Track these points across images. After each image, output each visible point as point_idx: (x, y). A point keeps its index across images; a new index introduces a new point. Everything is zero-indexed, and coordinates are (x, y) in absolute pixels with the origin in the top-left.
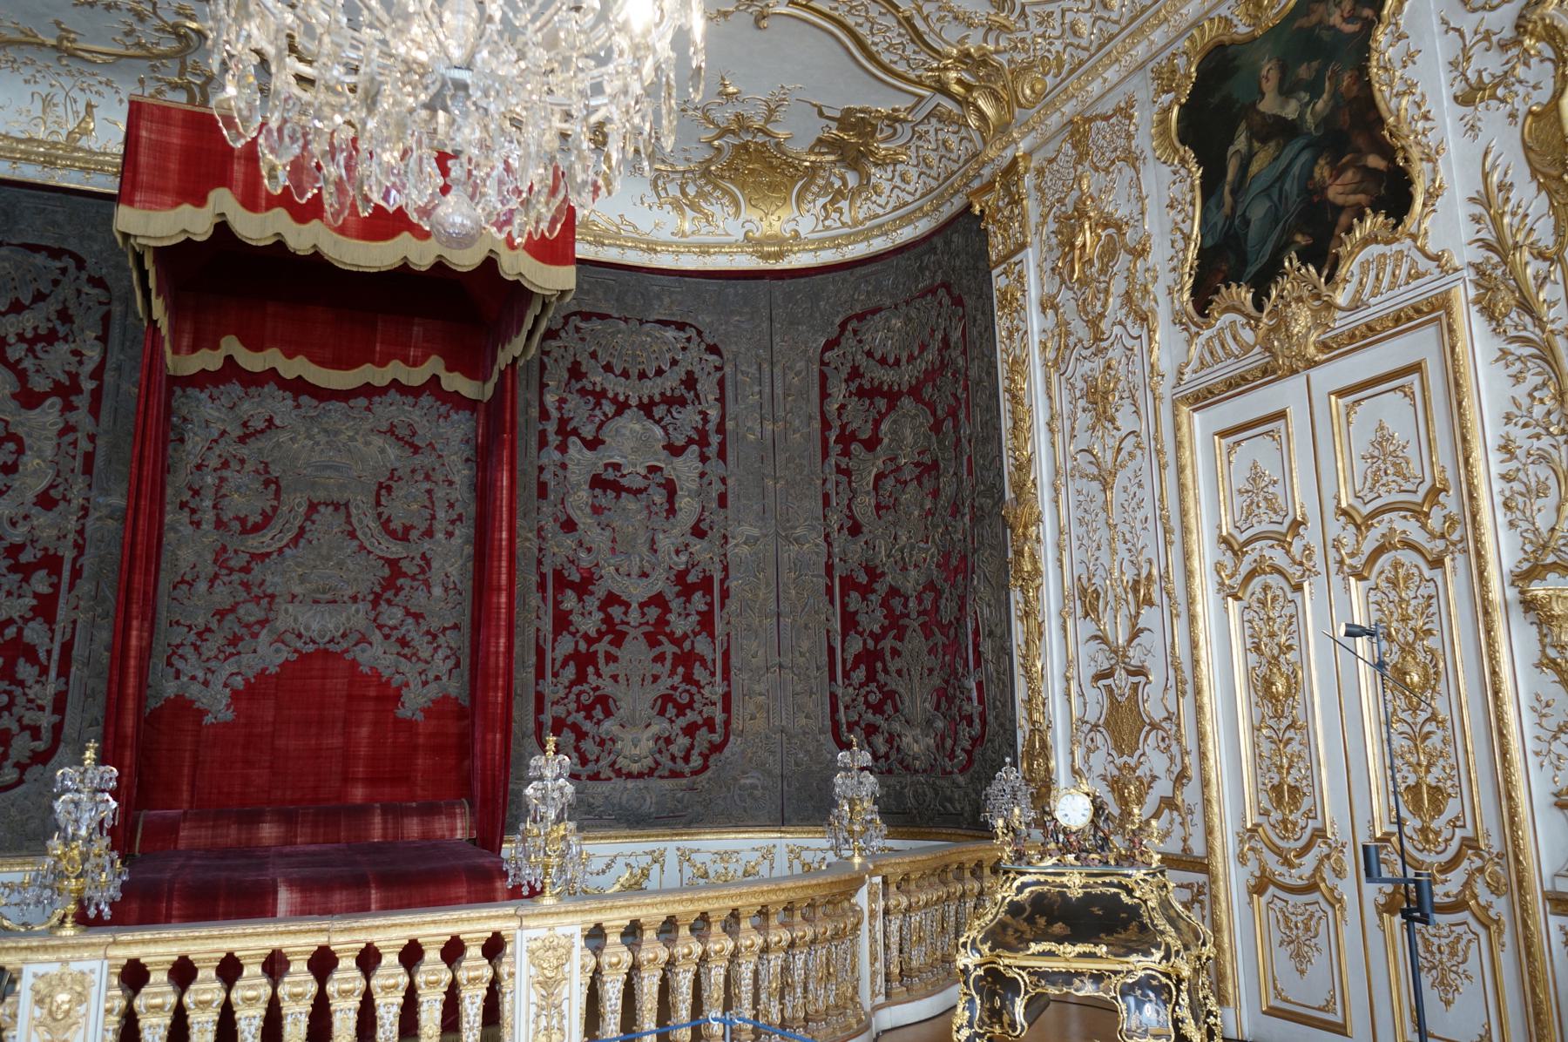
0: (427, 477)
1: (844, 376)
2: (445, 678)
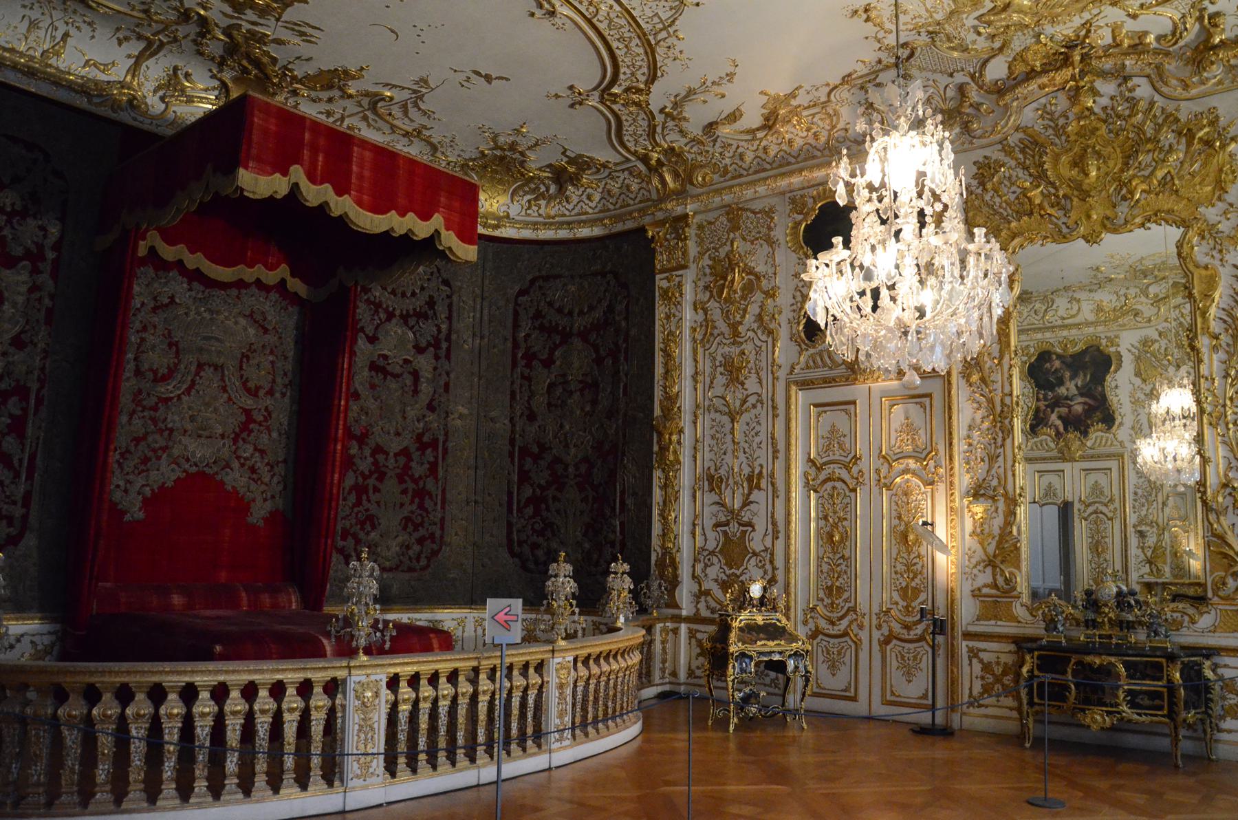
0: (272, 352)
1: (531, 315)
2: (277, 497)
